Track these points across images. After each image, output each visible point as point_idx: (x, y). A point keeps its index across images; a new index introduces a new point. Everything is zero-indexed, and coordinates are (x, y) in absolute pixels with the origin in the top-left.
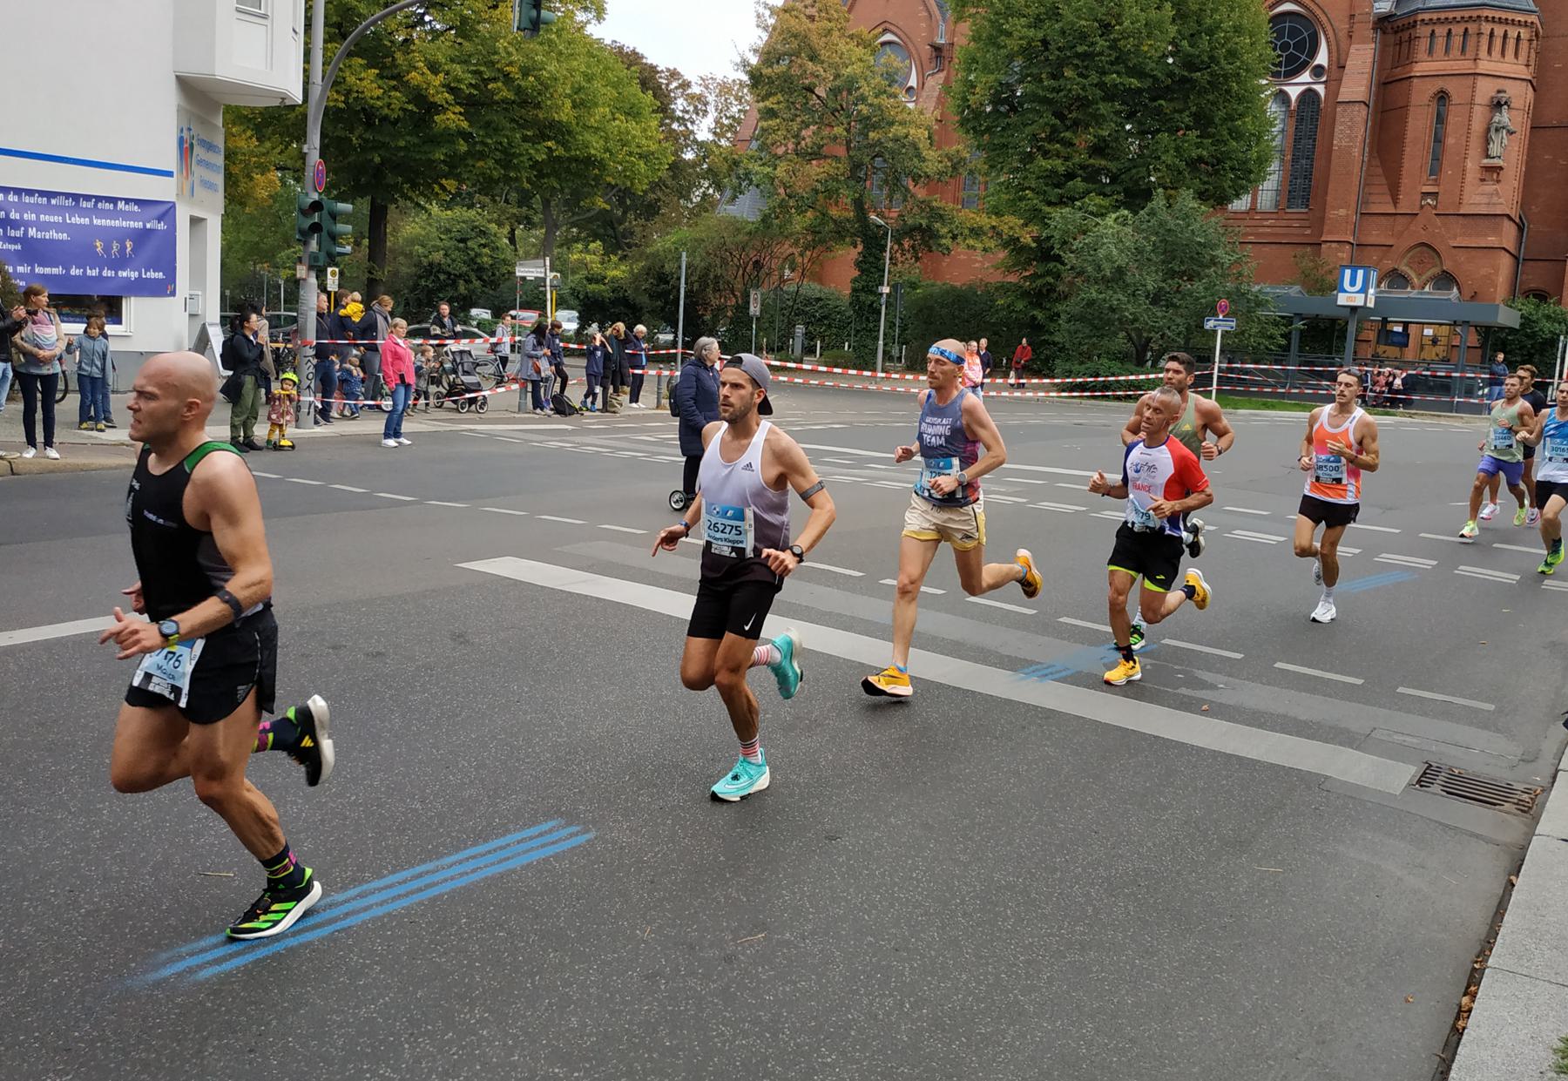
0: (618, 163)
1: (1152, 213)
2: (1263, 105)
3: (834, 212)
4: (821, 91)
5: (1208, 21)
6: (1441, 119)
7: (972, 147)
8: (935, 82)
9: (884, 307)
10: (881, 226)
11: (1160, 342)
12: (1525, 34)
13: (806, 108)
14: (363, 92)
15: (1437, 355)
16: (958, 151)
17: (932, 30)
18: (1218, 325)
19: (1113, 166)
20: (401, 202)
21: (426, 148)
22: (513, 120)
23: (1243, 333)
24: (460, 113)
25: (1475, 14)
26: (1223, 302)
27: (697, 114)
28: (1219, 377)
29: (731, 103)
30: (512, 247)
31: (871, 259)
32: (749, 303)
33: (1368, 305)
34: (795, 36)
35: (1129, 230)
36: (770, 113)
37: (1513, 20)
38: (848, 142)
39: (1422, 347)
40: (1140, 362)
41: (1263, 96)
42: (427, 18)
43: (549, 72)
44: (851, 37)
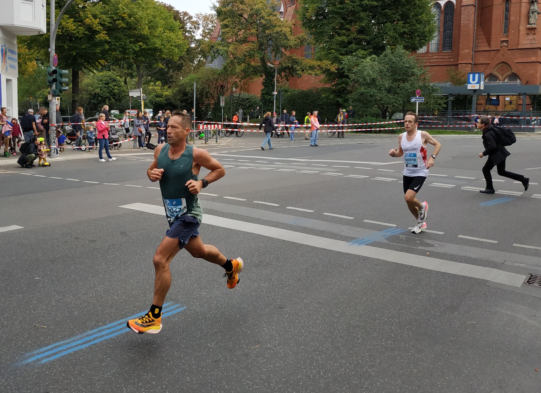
0: (167, 49)
1: (386, 56)
2: (430, 9)
3: (253, 64)
8: (291, 9)
9: (275, 100)
11: (392, 108)
13: (240, 23)
14: (68, 28)
15: (512, 108)
16: (303, 36)
19: (367, 38)
20: (85, 71)
22: (126, 35)
23: (427, 103)
24: (106, 34)
26: (418, 91)
27: (196, 29)
29: (209, 24)
30: (126, 85)
31: (269, 81)
32: (220, 101)
35: (377, 63)
36: (226, 26)
38: (257, 35)
39: (505, 106)
40: (384, 117)
41: (429, 5)
43: (139, 15)
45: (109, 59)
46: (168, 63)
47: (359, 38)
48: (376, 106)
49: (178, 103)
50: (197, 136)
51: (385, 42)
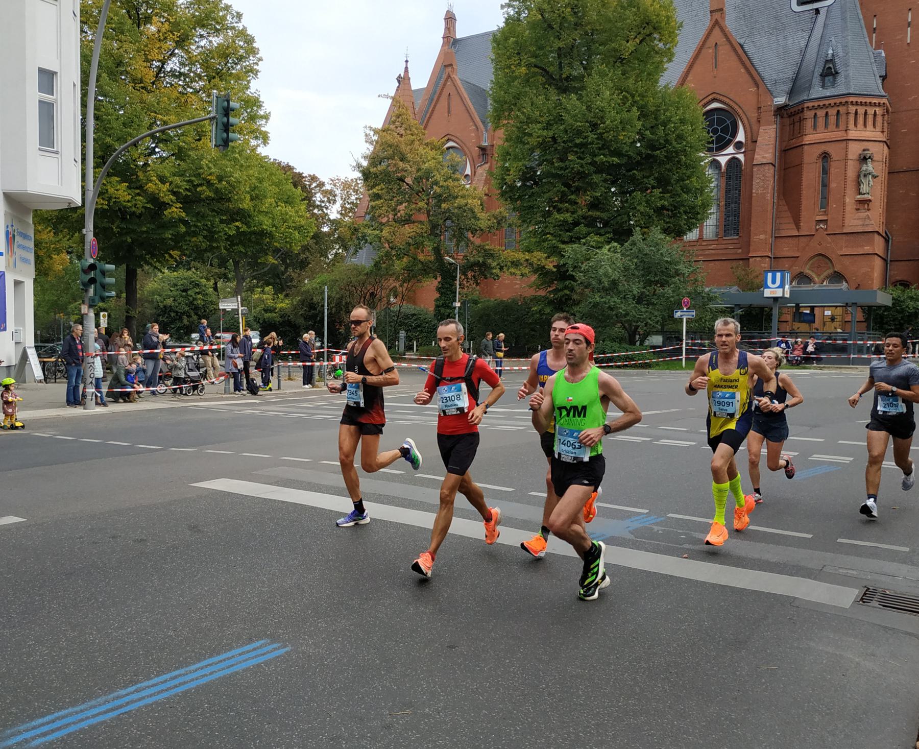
1: (634, 244)
3: (421, 257)
4: (409, 180)
5: (663, 117)
6: (825, 171)
7: (509, 210)
8: (482, 171)
10: (453, 263)
11: (645, 328)
12: (879, 111)
14: (119, 198)
16: (501, 213)
17: (479, 138)
18: (684, 315)
19: (604, 216)
20: (146, 267)
21: (160, 231)
22: (213, 210)
23: (701, 319)
24: (180, 208)
25: (844, 100)
26: (686, 299)
27: (330, 203)
28: (687, 349)
30: (216, 293)
31: (447, 286)
33: (786, 296)
34: (390, 146)
36: (377, 197)
37: (870, 103)
38: (428, 212)
39: (824, 324)
40: (632, 342)
41: (702, 163)
42: (157, 150)
43: (235, 178)
44: (427, 144)
45: (187, 249)
46: (285, 258)
47: (591, 216)
48: (619, 325)
49: (301, 321)
50: (330, 374)
51: (632, 222)
